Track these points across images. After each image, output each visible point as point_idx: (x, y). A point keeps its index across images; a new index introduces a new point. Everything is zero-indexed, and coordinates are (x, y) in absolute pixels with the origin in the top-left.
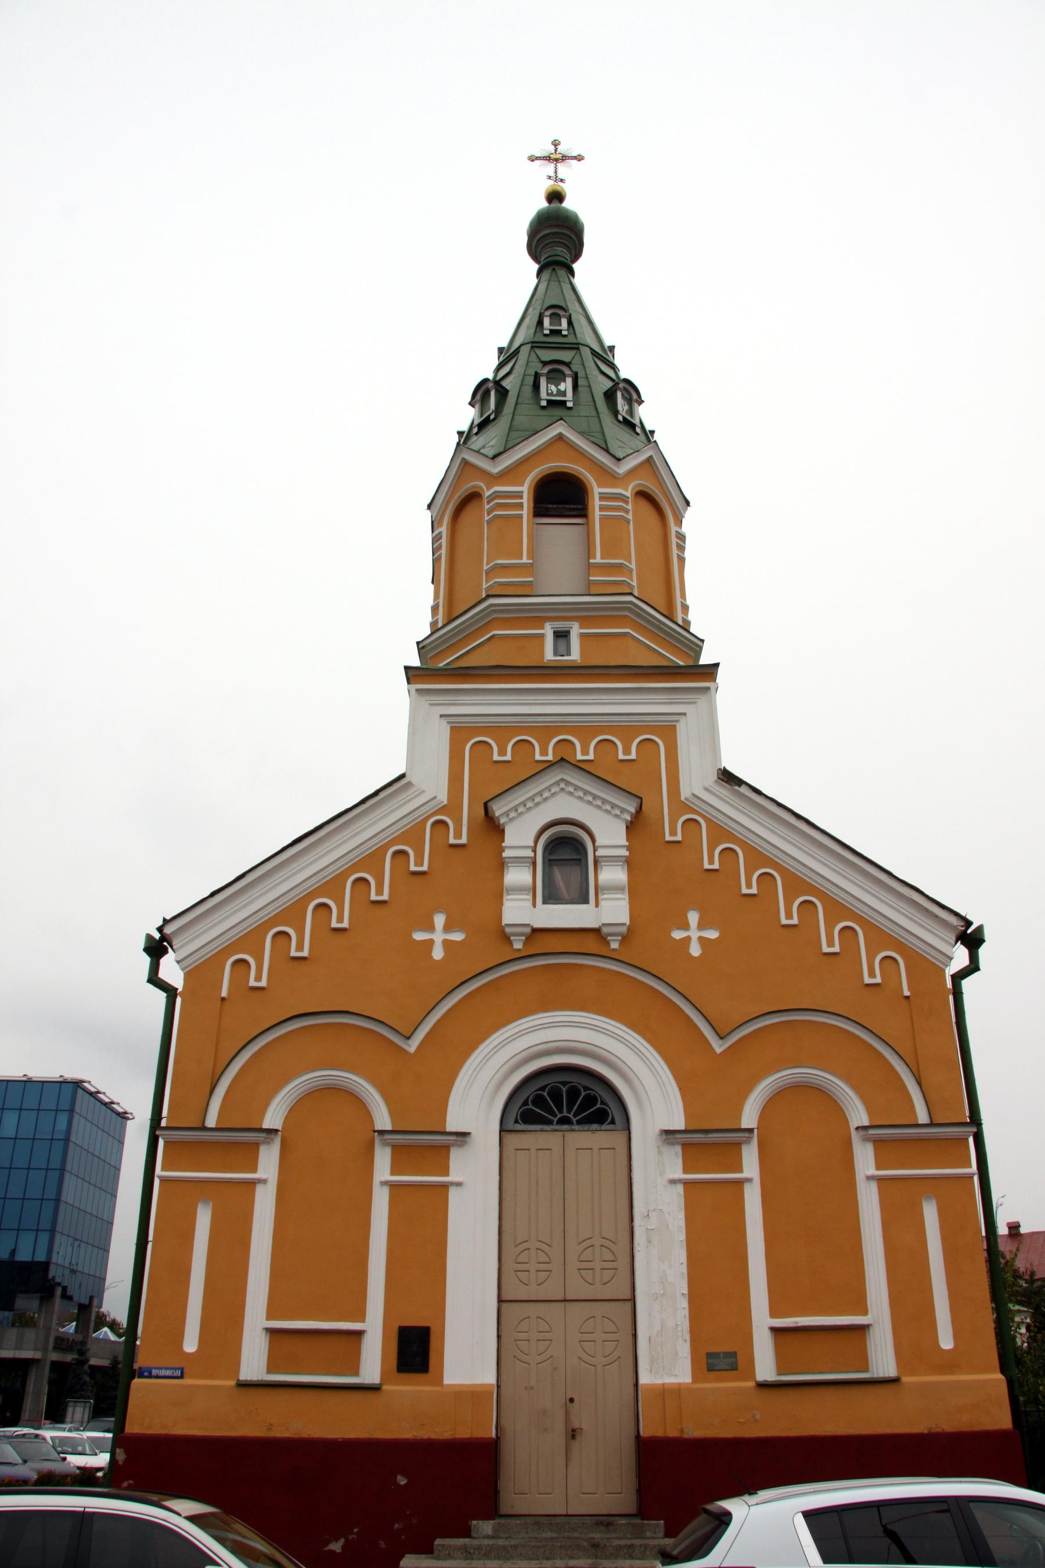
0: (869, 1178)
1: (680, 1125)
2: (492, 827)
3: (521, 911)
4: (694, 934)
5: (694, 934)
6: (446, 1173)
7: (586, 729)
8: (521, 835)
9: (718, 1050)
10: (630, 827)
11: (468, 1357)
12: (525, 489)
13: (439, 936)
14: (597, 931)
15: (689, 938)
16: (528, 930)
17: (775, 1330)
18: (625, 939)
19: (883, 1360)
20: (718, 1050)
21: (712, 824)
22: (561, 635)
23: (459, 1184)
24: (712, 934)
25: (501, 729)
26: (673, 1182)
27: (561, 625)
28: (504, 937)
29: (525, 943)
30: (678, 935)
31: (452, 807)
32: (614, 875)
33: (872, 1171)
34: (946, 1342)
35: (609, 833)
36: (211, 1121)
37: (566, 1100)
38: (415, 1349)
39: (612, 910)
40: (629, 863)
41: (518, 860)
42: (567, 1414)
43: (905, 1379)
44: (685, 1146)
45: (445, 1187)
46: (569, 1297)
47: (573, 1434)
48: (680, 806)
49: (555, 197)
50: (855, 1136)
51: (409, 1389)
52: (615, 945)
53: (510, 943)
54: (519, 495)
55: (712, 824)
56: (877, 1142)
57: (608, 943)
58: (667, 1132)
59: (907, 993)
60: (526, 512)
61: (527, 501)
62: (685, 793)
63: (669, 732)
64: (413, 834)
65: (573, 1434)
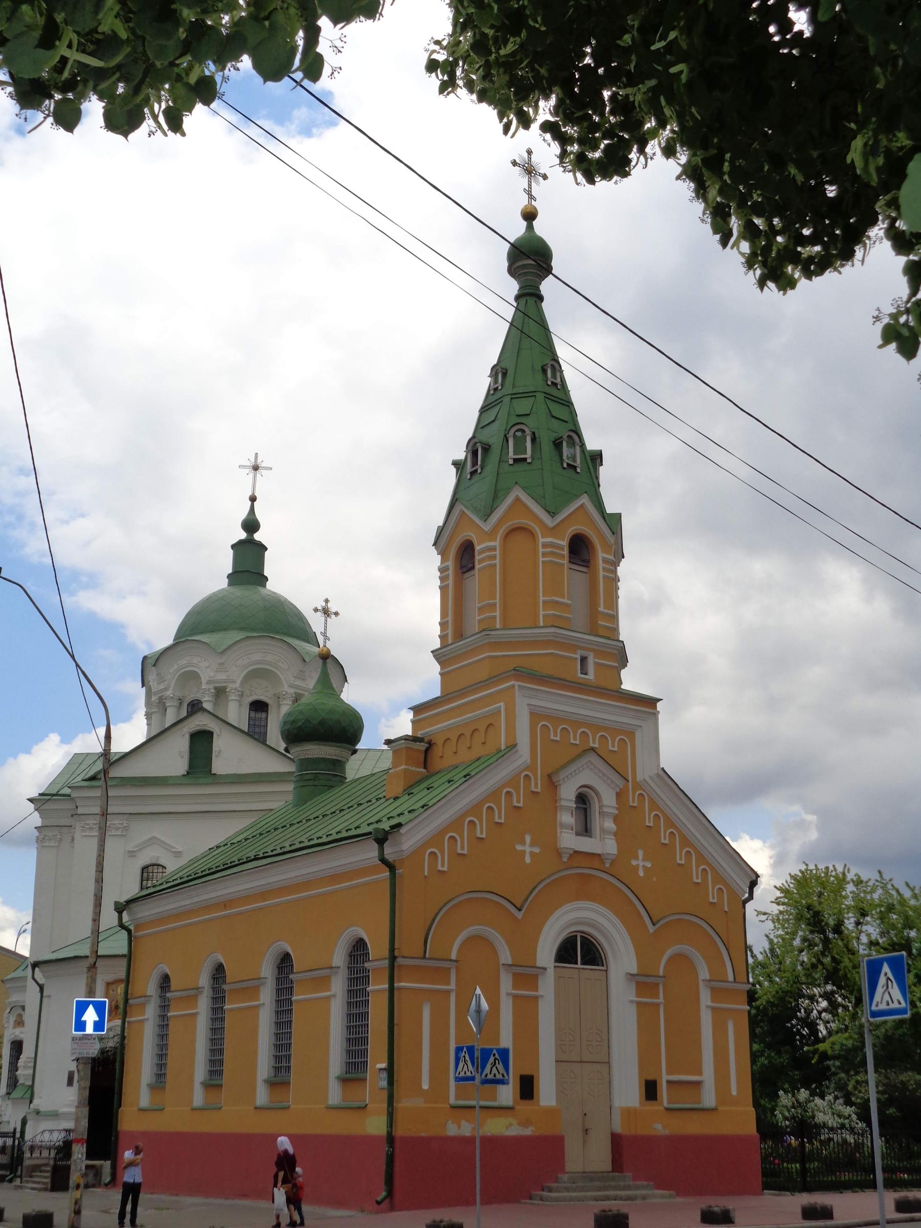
0: (707, 1007)
1: (636, 972)
2: (551, 782)
3: (569, 841)
4: (641, 863)
5: (641, 863)
6: (536, 990)
7: (596, 727)
8: (568, 793)
9: (651, 931)
10: (617, 794)
11: (547, 1093)
12: (565, 543)
13: (527, 848)
14: (599, 855)
15: (638, 865)
16: (572, 852)
17: (669, 1082)
18: (613, 862)
19: (709, 1099)
20: (651, 931)
21: (652, 801)
22: (583, 660)
23: (542, 996)
24: (649, 865)
25: (556, 719)
26: (632, 1002)
27: (585, 653)
28: (559, 853)
29: (569, 859)
30: (634, 863)
31: (531, 767)
32: (610, 825)
33: (709, 1004)
34: (734, 1092)
35: (608, 799)
36: (427, 956)
37: (580, 951)
38: (527, 1088)
39: (610, 847)
40: (616, 819)
41: (567, 808)
42: (583, 1120)
43: (720, 1108)
44: (638, 983)
45: (536, 998)
46: (584, 1059)
47: (586, 1131)
48: (637, 786)
49: (530, 216)
50: (701, 983)
51: (525, 1107)
52: (607, 865)
53: (561, 857)
54: (561, 548)
55: (652, 801)
56: (713, 989)
57: (604, 864)
58: (632, 975)
59: (726, 909)
60: (566, 561)
61: (566, 552)
62: (639, 778)
63: (631, 735)
64: (513, 781)
65: (586, 1131)
